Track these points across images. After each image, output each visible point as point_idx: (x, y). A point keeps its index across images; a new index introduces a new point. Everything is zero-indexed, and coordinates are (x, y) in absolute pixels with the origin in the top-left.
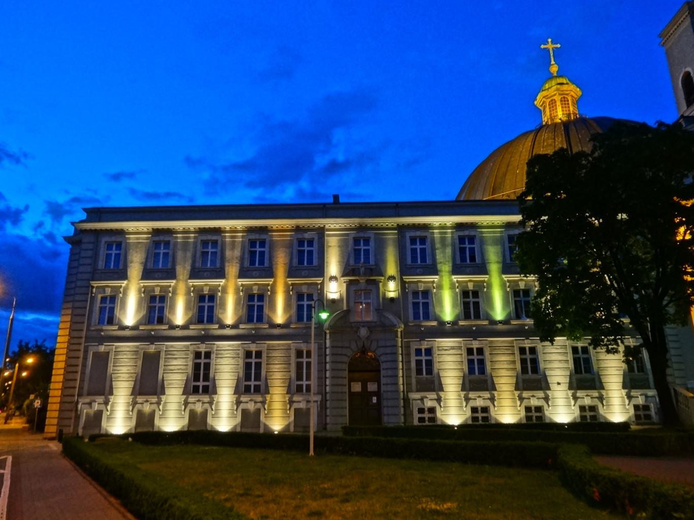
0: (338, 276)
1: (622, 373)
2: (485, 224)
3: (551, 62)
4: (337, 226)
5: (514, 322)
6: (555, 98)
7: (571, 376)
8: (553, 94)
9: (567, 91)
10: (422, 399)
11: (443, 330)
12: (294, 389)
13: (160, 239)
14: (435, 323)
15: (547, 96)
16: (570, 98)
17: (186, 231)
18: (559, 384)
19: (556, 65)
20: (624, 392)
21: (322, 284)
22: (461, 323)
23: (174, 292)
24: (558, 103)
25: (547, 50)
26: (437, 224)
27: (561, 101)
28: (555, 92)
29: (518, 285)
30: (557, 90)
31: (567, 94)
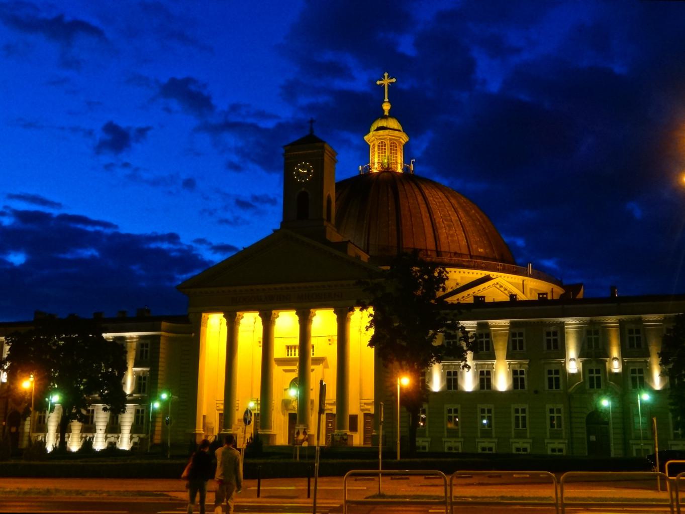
1: (131, 424)
3: (385, 99)
7: (107, 426)
9: (384, 135)
10: (37, 437)
16: (388, 143)
18: (101, 430)
25: (382, 87)
27: (379, 146)
31: (384, 139)
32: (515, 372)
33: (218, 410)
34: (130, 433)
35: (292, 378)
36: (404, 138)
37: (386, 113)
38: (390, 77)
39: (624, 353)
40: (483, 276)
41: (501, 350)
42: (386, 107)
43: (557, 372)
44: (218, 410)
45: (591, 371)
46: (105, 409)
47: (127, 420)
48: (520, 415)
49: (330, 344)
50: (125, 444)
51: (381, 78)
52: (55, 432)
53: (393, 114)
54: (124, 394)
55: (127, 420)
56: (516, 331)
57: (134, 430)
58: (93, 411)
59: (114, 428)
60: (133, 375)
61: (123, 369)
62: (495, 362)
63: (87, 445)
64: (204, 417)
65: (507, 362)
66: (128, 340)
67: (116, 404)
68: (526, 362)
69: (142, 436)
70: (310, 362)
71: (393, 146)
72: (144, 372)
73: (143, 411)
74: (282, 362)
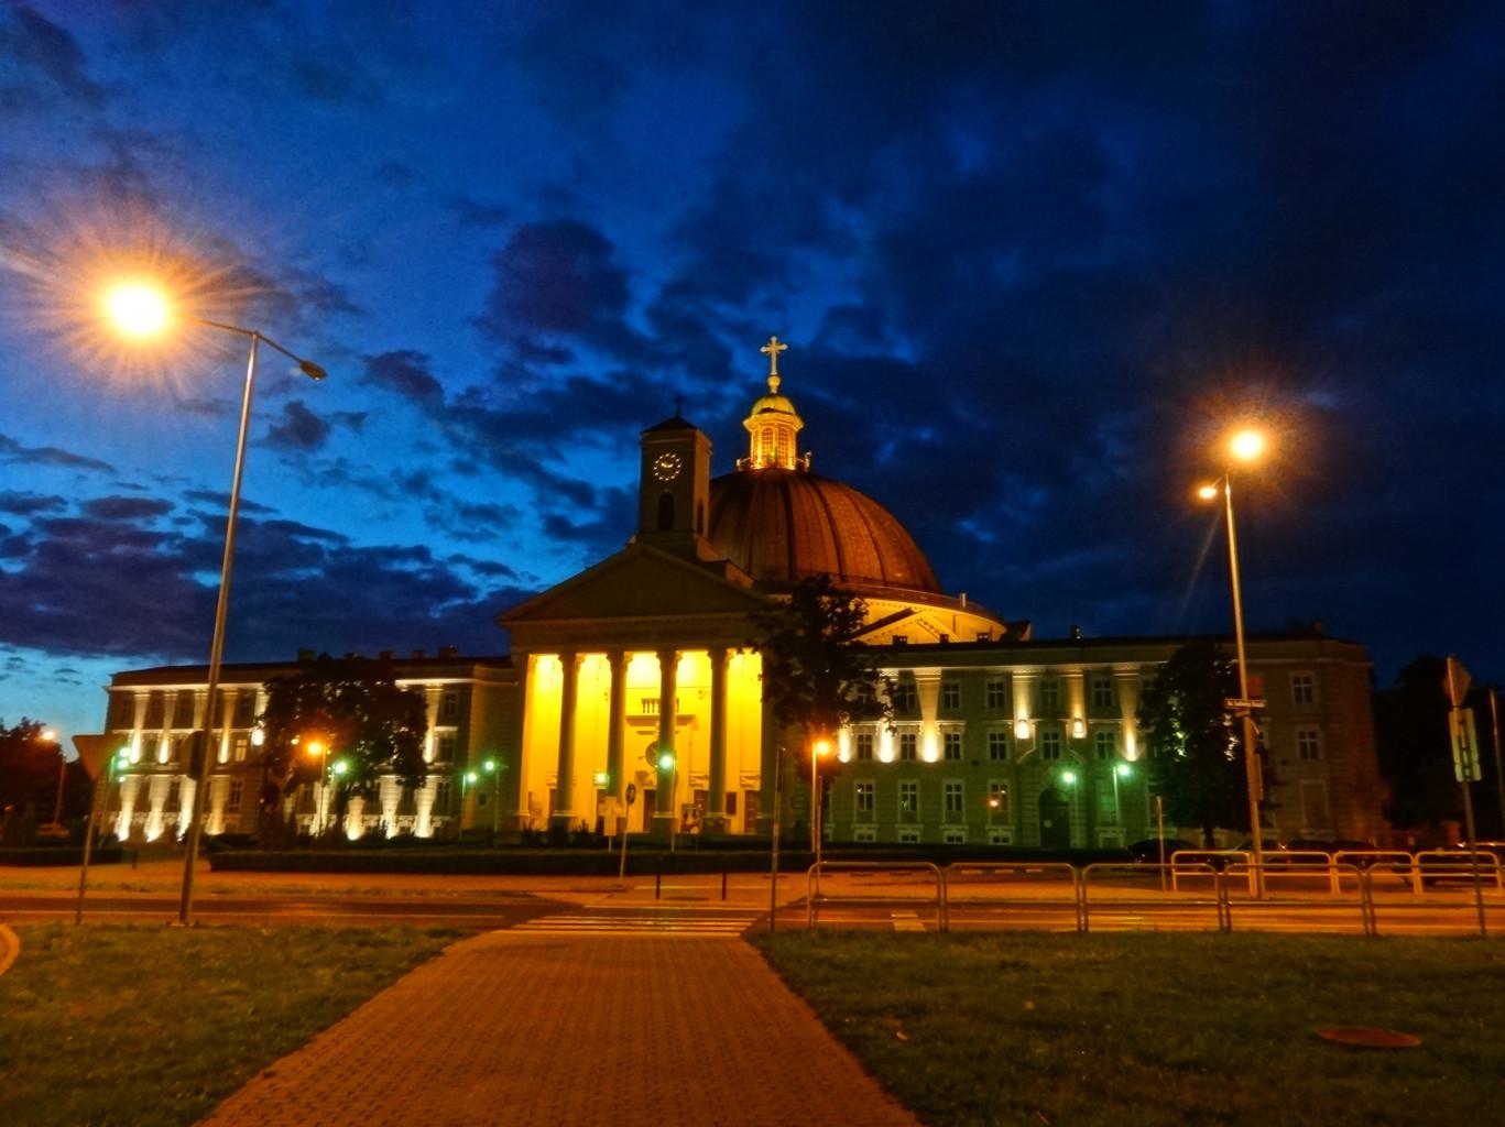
12: (229, 809)
13: (156, 697)
16: (775, 429)
17: (172, 692)
23: (162, 738)
25: (768, 356)
27: (764, 434)
31: (773, 424)
32: (948, 737)
33: (549, 785)
35: (648, 745)
36: (798, 425)
37: (774, 391)
38: (780, 342)
39: (1089, 713)
40: (902, 609)
41: (929, 707)
43: (1002, 737)
44: (549, 785)
45: (1046, 736)
46: (399, 783)
47: (426, 798)
48: (954, 793)
49: (701, 698)
50: (423, 828)
51: (767, 342)
53: (782, 392)
54: (423, 764)
55: (426, 798)
56: (948, 681)
57: (435, 811)
58: (379, 785)
59: (407, 807)
60: (434, 736)
61: (421, 728)
62: (921, 723)
64: (530, 794)
65: (938, 723)
67: (412, 774)
68: (962, 723)
69: (447, 818)
70: (674, 720)
71: (783, 435)
72: (450, 733)
73: (447, 785)
74: (635, 721)
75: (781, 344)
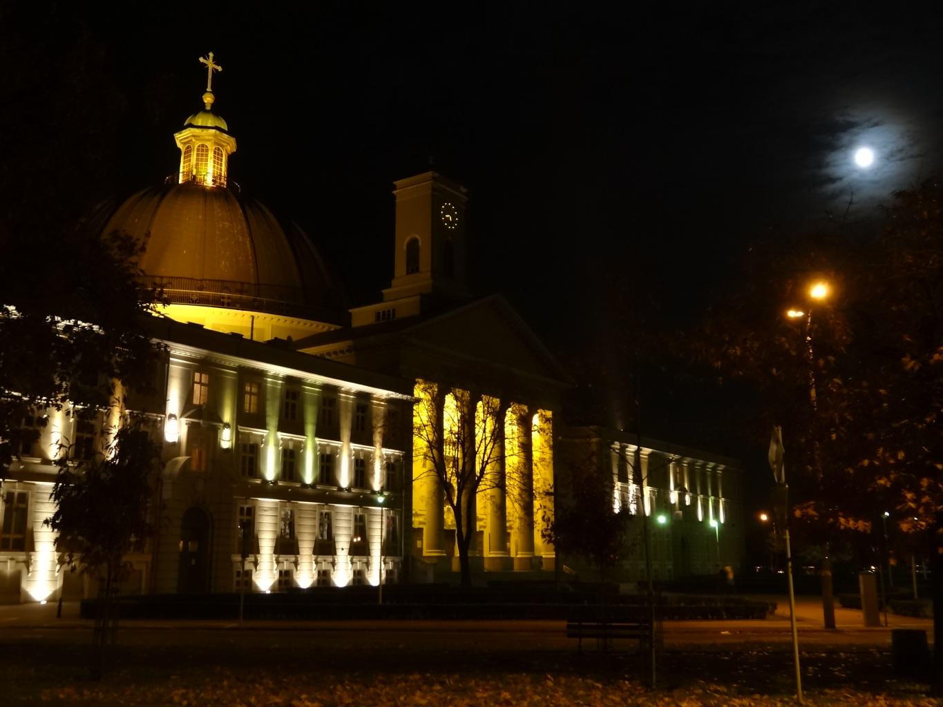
0: (230, 424)
2: (309, 381)
4: (183, 354)
5: (319, 487)
6: (208, 144)
8: (207, 137)
11: (266, 490)
14: (259, 482)
15: (198, 136)
19: (212, 95)
20: (274, 556)
21: (162, 422)
22: (280, 484)
24: (211, 154)
26: (271, 373)
28: (211, 138)
29: (325, 450)
30: (215, 136)
34: (350, 554)
37: (208, 108)
42: (208, 99)
52: (272, 552)
53: (216, 111)
60: (350, 456)
63: (324, 577)
66: (374, 401)
75: (208, 56)
